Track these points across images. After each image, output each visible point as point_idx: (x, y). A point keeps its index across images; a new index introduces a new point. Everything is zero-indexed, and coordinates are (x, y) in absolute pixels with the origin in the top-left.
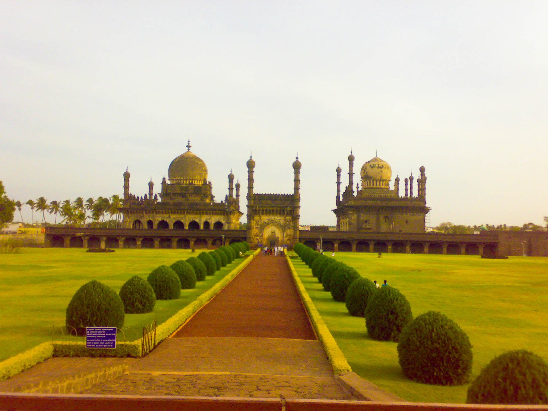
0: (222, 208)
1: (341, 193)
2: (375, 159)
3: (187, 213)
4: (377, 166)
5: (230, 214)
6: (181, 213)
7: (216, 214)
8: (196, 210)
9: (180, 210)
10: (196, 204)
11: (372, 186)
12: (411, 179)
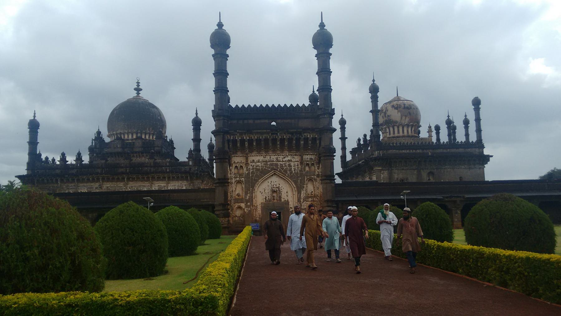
0: (183, 169)
1: (349, 149)
2: (398, 99)
3: (128, 179)
4: (403, 106)
6: (118, 180)
7: (174, 179)
10: (142, 165)
11: (396, 134)
12: (449, 123)
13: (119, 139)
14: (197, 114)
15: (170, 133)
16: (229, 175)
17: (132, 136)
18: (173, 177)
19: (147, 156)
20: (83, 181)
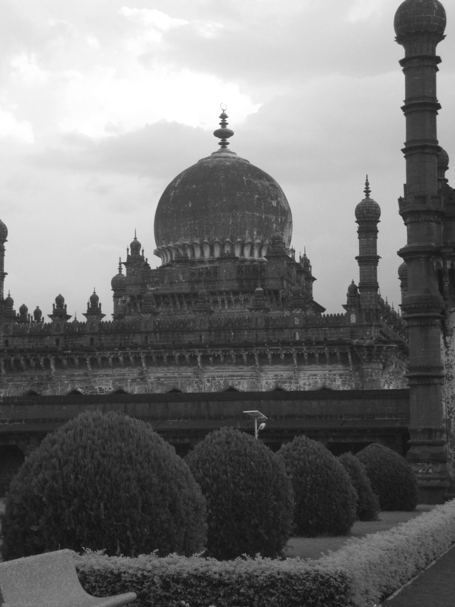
5: (370, 361)
7: (311, 360)
8: (236, 347)
9: (179, 348)
10: (236, 325)
13: (182, 261)
14: (367, 192)
15: (300, 243)
16: (444, 358)
17: (212, 253)
18: (311, 356)
19: (246, 301)
20: (104, 363)
